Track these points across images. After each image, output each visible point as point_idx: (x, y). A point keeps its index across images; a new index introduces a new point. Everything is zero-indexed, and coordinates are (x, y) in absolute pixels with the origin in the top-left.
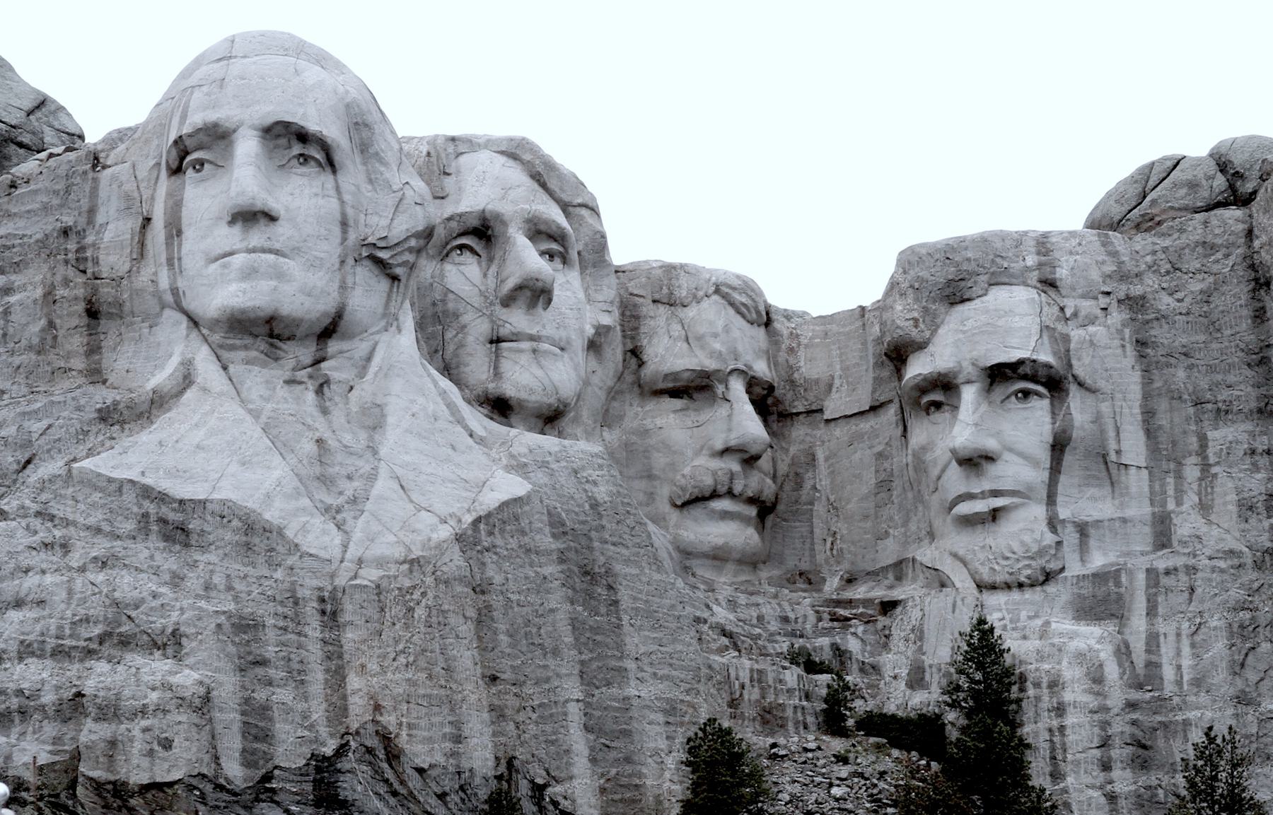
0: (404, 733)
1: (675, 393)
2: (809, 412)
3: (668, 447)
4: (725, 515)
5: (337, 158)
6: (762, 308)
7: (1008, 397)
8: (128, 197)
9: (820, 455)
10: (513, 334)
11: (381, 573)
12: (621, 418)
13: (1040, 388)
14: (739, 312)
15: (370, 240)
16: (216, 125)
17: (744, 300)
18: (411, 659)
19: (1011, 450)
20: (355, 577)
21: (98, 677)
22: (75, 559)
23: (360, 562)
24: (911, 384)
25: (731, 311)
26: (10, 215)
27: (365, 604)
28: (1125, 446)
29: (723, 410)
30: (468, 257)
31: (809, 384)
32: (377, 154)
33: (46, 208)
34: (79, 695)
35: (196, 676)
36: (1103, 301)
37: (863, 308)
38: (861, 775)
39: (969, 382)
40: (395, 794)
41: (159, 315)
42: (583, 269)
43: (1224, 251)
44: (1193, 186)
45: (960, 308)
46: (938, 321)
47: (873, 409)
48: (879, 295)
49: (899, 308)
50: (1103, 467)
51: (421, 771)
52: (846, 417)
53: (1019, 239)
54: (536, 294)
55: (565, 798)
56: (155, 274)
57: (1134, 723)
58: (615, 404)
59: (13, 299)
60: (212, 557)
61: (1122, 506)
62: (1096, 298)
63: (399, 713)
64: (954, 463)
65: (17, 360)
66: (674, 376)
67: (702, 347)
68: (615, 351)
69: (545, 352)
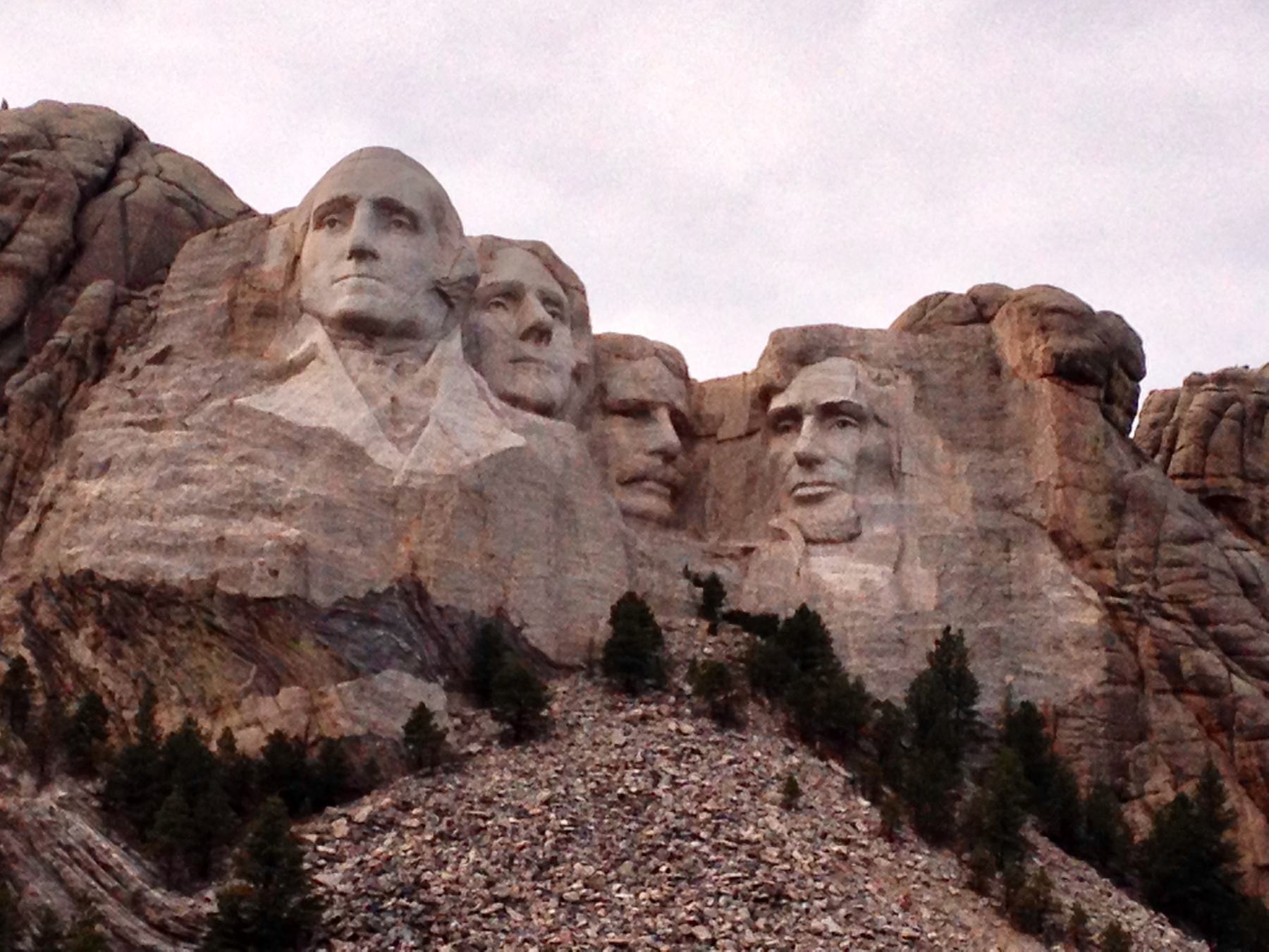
0: (431, 582)
1: (625, 413)
3: (617, 445)
4: (650, 491)
5: (421, 224)
9: (713, 462)
11: (425, 481)
13: (853, 421)
16: (345, 197)
21: (235, 529)
22: (230, 456)
23: (411, 473)
25: (664, 369)
26: (213, 255)
28: (905, 460)
29: (650, 428)
30: (500, 310)
31: (712, 417)
33: (236, 251)
34: (221, 539)
35: (298, 532)
37: (745, 374)
38: (723, 643)
39: (809, 413)
40: (421, 621)
41: (300, 317)
44: (956, 310)
45: (810, 369)
48: (755, 366)
51: (439, 609)
52: (731, 439)
53: (846, 331)
54: (540, 334)
57: (900, 629)
59: (208, 303)
60: (315, 464)
61: (901, 498)
64: (797, 466)
66: (624, 402)
68: (590, 384)
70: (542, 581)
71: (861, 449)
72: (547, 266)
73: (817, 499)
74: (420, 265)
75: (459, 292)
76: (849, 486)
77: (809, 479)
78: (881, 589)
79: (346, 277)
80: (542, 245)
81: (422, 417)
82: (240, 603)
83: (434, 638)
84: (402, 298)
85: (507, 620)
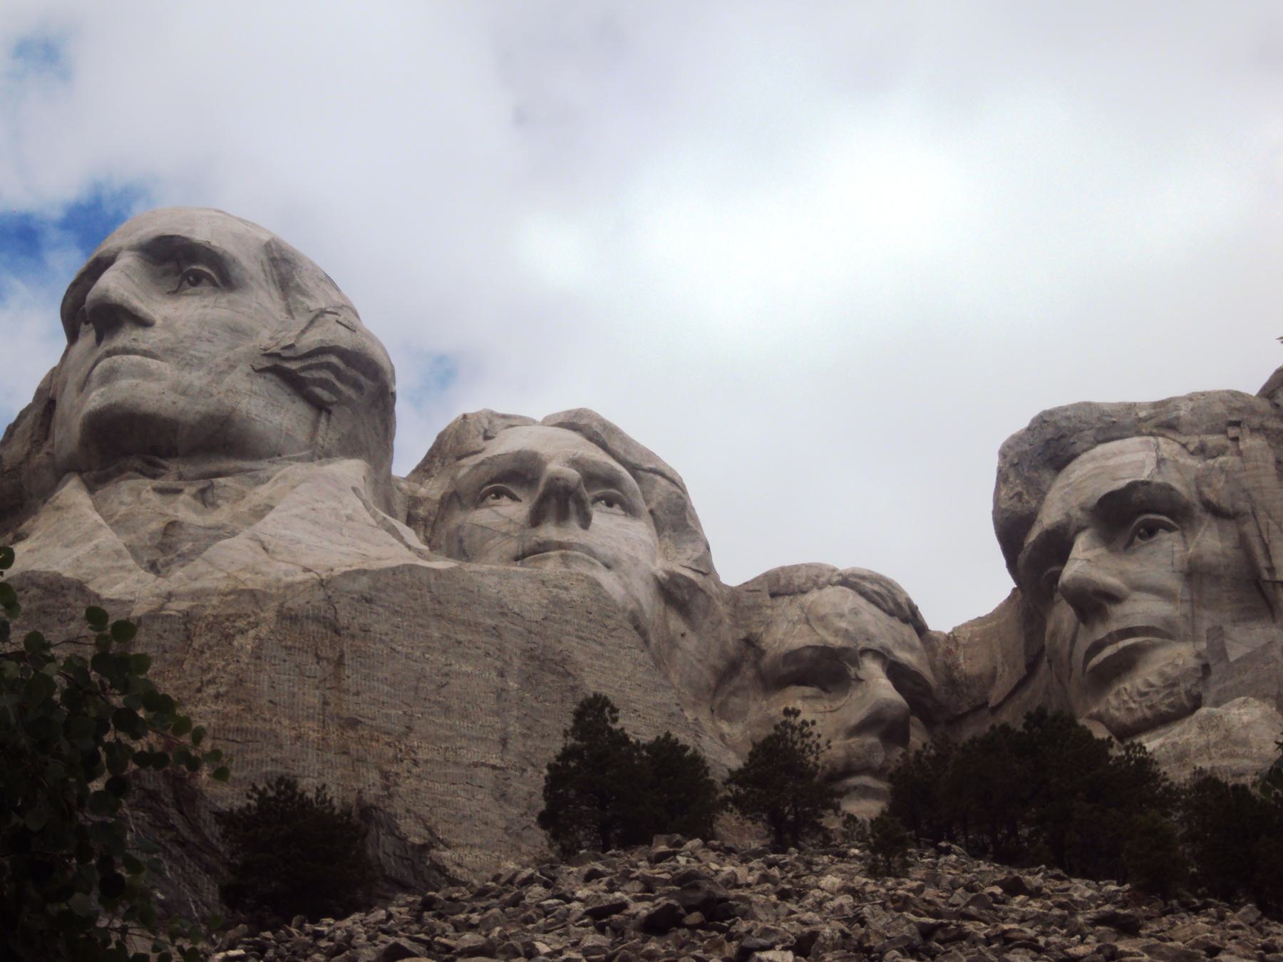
2: (977, 709)
4: (866, 792)
5: (235, 273)
6: (902, 600)
7: (1130, 543)
10: (539, 544)
12: (743, 714)
13: (1165, 518)
15: (276, 350)
17: (876, 588)
18: (222, 690)
19: (1138, 588)
25: (862, 602)
27: (165, 635)
29: (856, 694)
30: (505, 500)
32: (298, 286)
36: (1233, 432)
39: (1080, 529)
40: (183, 844)
42: (659, 527)
47: (1032, 667)
52: (1010, 696)
55: (459, 865)
58: (737, 700)
62: (1225, 432)
64: (1082, 625)
66: (793, 656)
67: (826, 627)
69: (577, 557)
70: (482, 772)
71: (1189, 561)
72: (590, 439)
73: (1126, 663)
74: (236, 331)
75: (325, 374)
77: (1101, 633)
78: (1246, 726)
80: (579, 413)
83: (208, 870)
84: (196, 378)
85: (392, 830)
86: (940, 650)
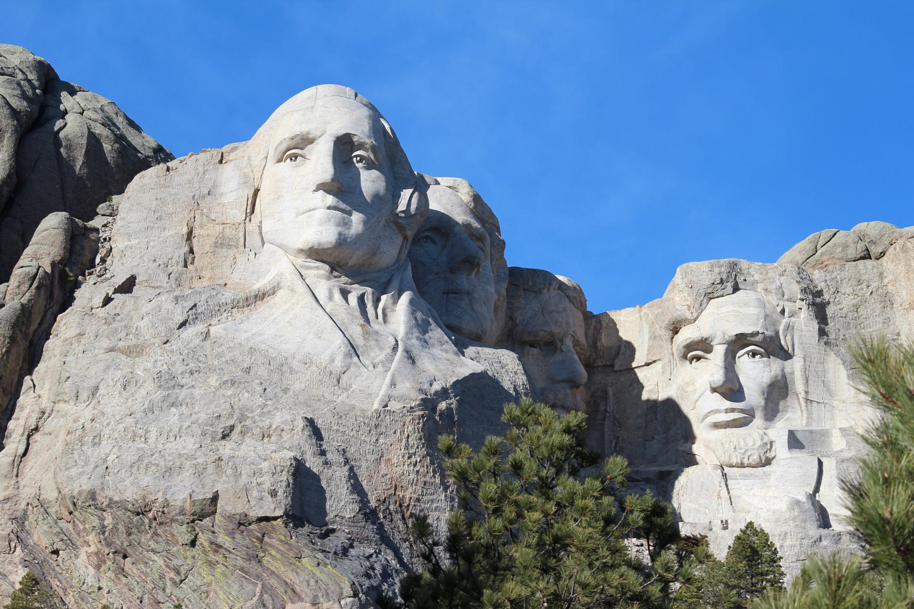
1: (532, 346)
2: (605, 366)
8: (245, 176)
9: (611, 392)
14: (571, 301)
20: (386, 406)
24: (684, 343)
29: (558, 357)
35: (292, 454)
36: (799, 304)
43: (865, 283)
44: (845, 246)
46: (703, 307)
49: (678, 299)
50: (796, 401)
56: (261, 222)
63: (410, 490)
65: (170, 269)
68: (502, 315)
76: (759, 414)
79: (310, 210)
81: (393, 342)
82: (242, 523)
86: (592, 327)
